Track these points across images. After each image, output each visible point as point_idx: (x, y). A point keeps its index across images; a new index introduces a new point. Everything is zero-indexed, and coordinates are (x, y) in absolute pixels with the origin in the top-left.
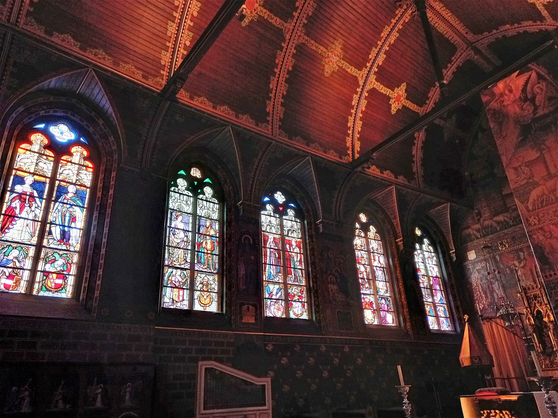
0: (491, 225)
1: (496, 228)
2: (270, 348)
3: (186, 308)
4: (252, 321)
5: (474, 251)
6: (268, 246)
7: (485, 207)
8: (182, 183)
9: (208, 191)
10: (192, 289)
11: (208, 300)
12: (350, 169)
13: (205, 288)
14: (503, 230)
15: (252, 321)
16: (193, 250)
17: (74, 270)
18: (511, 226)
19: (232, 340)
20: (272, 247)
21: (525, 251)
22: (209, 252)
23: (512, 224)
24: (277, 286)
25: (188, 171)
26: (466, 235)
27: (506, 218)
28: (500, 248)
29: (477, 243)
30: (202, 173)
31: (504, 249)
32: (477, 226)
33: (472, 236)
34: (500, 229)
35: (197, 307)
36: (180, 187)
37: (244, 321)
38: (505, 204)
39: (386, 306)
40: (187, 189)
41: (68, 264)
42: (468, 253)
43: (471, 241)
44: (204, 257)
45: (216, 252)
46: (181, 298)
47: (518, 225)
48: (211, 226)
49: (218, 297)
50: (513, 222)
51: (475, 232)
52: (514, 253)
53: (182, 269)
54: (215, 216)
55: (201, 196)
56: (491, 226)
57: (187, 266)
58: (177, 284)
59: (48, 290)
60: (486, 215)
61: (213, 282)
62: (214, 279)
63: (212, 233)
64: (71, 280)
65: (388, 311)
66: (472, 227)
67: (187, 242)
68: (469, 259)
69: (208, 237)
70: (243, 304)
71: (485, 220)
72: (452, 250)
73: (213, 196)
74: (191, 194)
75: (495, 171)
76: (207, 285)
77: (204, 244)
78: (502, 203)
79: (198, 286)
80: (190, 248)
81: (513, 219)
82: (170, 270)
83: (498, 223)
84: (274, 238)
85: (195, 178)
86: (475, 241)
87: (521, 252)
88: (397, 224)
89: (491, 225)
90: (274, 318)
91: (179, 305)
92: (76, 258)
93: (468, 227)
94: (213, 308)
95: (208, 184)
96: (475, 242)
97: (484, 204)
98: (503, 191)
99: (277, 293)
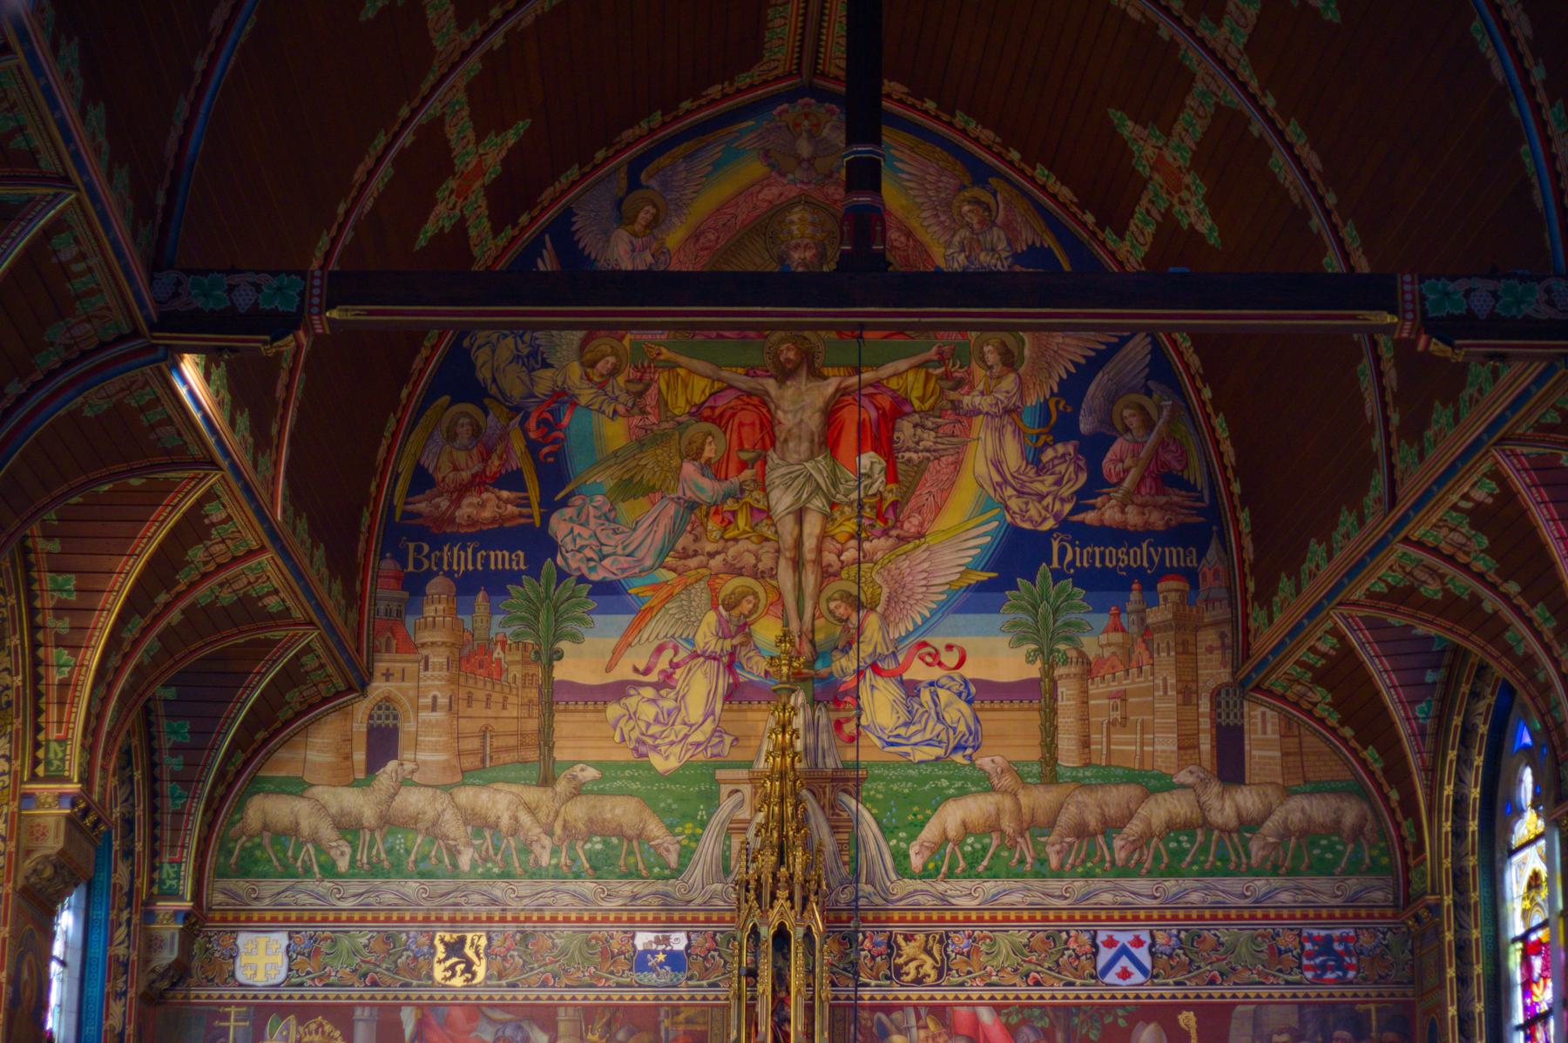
0: (435, 824)
1: (454, 853)
5: (281, 939)
7: (434, 708)
12: (147, 318)
14: (487, 875)
18: (536, 873)
21: (562, 1027)
23: (545, 859)
26: (265, 827)
27: (525, 818)
28: (439, 972)
29: (319, 897)
31: (458, 981)
32: (357, 802)
33: (300, 845)
34: (474, 865)
38: (546, 738)
42: (243, 939)
43: (287, 872)
47: (577, 876)
50: (555, 852)
51: (327, 832)
52: (505, 1023)
56: (434, 832)
60: (421, 756)
66: (323, 793)
68: (241, 976)
71: (405, 782)
72: (175, 895)
75: (559, 526)
78: (532, 725)
81: (558, 830)
83: (479, 824)
86: (310, 884)
87: (544, 1028)
88: (64, 685)
89: (435, 824)
93: (297, 787)
96: (309, 893)
97: (435, 684)
98: (560, 655)
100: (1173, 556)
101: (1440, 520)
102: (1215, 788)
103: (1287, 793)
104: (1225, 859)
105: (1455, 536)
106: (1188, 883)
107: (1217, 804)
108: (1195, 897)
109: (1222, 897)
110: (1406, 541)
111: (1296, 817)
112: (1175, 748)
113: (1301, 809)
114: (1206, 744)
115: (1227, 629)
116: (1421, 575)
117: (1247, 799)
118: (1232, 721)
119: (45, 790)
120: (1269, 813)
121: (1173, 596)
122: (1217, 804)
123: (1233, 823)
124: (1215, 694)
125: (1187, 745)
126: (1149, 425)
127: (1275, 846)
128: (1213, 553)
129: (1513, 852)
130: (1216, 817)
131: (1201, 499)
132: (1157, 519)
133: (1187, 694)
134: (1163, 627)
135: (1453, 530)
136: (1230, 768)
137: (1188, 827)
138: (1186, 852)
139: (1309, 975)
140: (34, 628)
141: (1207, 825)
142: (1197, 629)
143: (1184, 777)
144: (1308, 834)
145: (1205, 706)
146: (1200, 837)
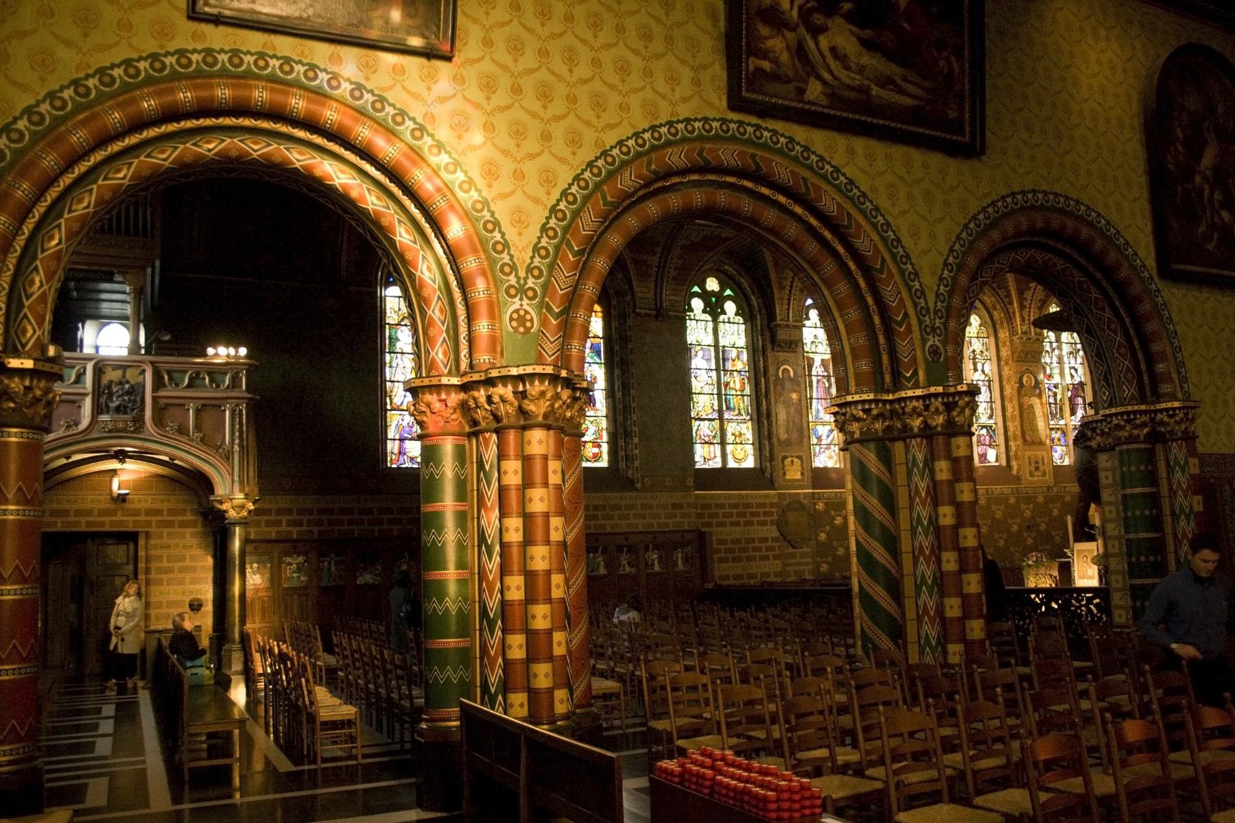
2: (820, 506)
3: (719, 465)
4: (798, 476)
6: (814, 373)
8: (697, 304)
9: (730, 307)
10: (723, 443)
11: (743, 453)
13: (738, 440)
15: (798, 476)
16: (719, 394)
17: (605, 438)
19: (775, 501)
20: (820, 373)
22: (739, 393)
24: (828, 428)
25: (702, 285)
30: (720, 283)
35: (732, 464)
36: (695, 312)
37: (787, 477)
39: (988, 438)
40: (704, 311)
41: (599, 432)
44: (734, 402)
45: (747, 391)
46: (712, 456)
48: (738, 357)
49: (754, 449)
53: (709, 420)
54: (741, 341)
55: (722, 317)
57: (715, 416)
58: (707, 439)
59: (588, 460)
61: (747, 431)
62: (747, 428)
63: (739, 366)
64: (605, 448)
65: (990, 445)
67: (713, 385)
69: (735, 373)
70: (785, 458)
73: (737, 314)
74: (709, 318)
76: (741, 434)
77: (732, 385)
79: (730, 438)
80: (715, 392)
82: (698, 423)
84: (823, 361)
85: (713, 293)
90: (825, 469)
91: (711, 462)
92: (604, 423)
94: (750, 463)
95: (729, 298)
99: (828, 436)
119: (1015, 338)
140: (1003, 302)
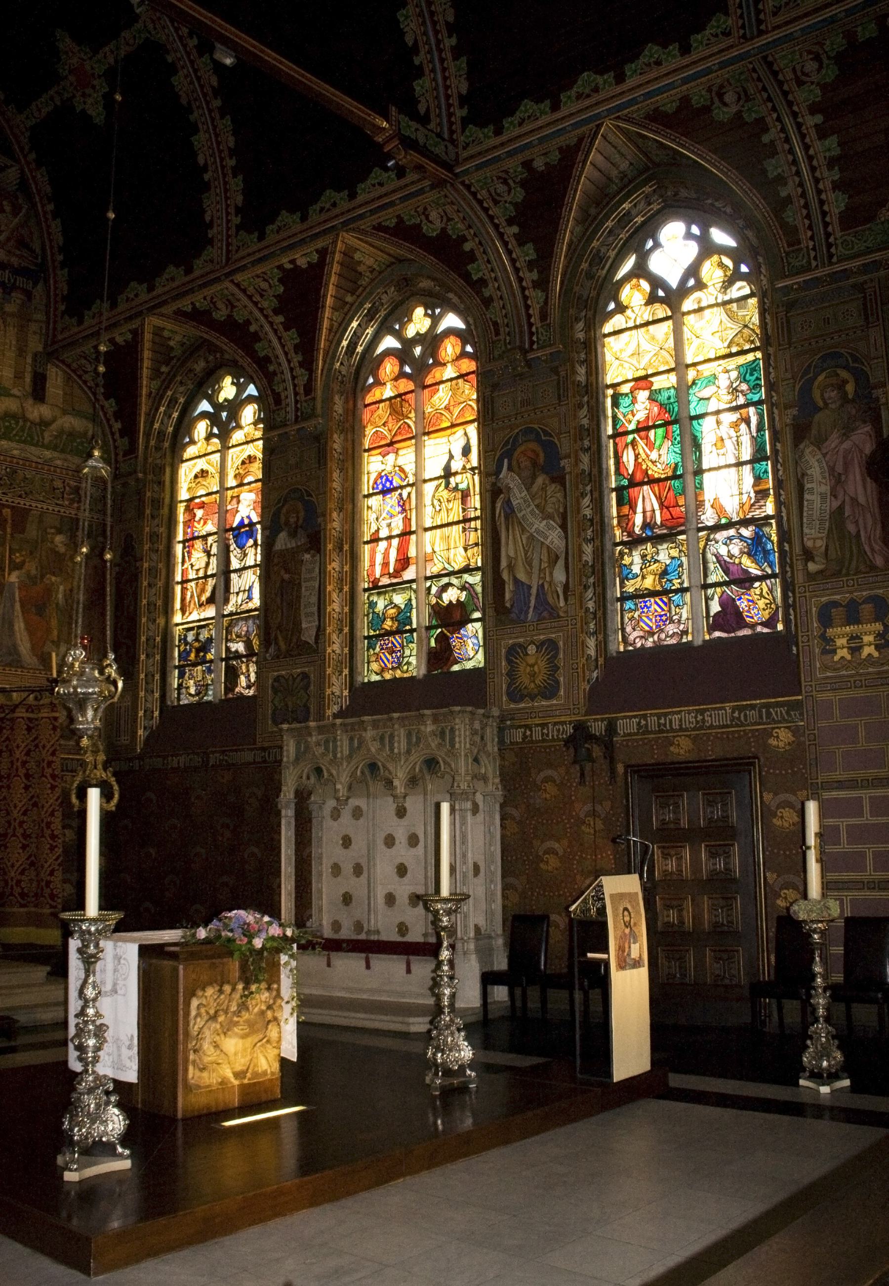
100: (20, 281)
101: (264, 273)
102: (30, 401)
103: (65, 412)
104: (33, 439)
105: (264, 285)
106: (13, 445)
107: (30, 409)
108: (16, 452)
109: (29, 455)
110: (232, 281)
111: (67, 425)
112: (12, 376)
113: (70, 422)
114: (28, 379)
115: (44, 326)
116: (220, 305)
117: (45, 411)
118: (41, 370)
120: (54, 420)
121: (18, 301)
122: (30, 409)
123: (38, 420)
124: (35, 355)
125: (19, 376)
126: (15, 214)
127: (56, 437)
128: (40, 287)
129: (183, 461)
130: (30, 416)
131: (36, 258)
132: (15, 261)
133: (21, 352)
134: (12, 315)
135: (265, 280)
136: (39, 393)
137: (14, 416)
138: (13, 429)
139: (67, 503)
141: (26, 420)
142: (29, 320)
143: (15, 391)
144: (72, 435)
145: (29, 360)
146: (21, 423)
